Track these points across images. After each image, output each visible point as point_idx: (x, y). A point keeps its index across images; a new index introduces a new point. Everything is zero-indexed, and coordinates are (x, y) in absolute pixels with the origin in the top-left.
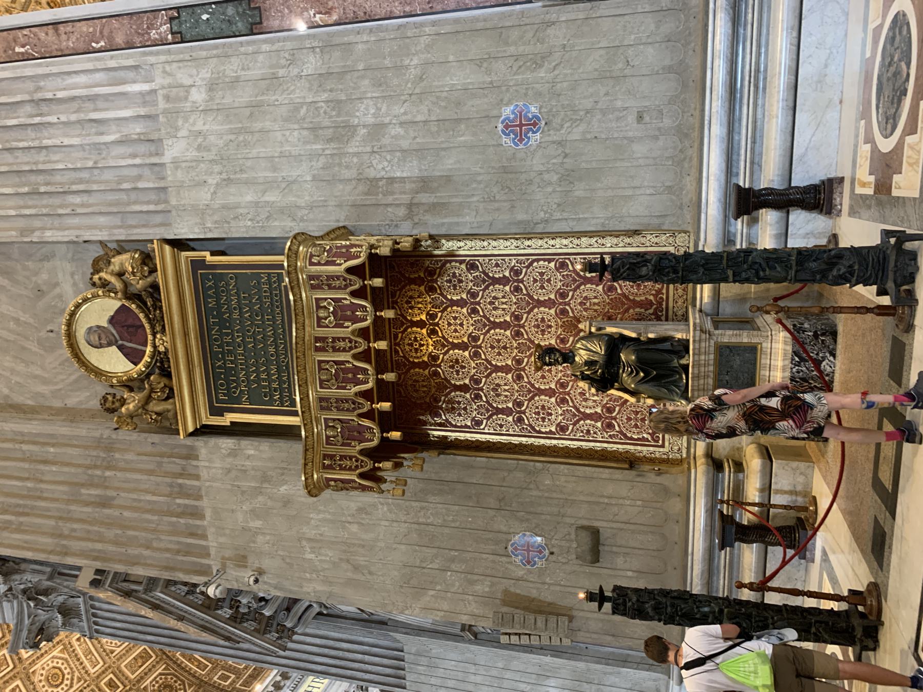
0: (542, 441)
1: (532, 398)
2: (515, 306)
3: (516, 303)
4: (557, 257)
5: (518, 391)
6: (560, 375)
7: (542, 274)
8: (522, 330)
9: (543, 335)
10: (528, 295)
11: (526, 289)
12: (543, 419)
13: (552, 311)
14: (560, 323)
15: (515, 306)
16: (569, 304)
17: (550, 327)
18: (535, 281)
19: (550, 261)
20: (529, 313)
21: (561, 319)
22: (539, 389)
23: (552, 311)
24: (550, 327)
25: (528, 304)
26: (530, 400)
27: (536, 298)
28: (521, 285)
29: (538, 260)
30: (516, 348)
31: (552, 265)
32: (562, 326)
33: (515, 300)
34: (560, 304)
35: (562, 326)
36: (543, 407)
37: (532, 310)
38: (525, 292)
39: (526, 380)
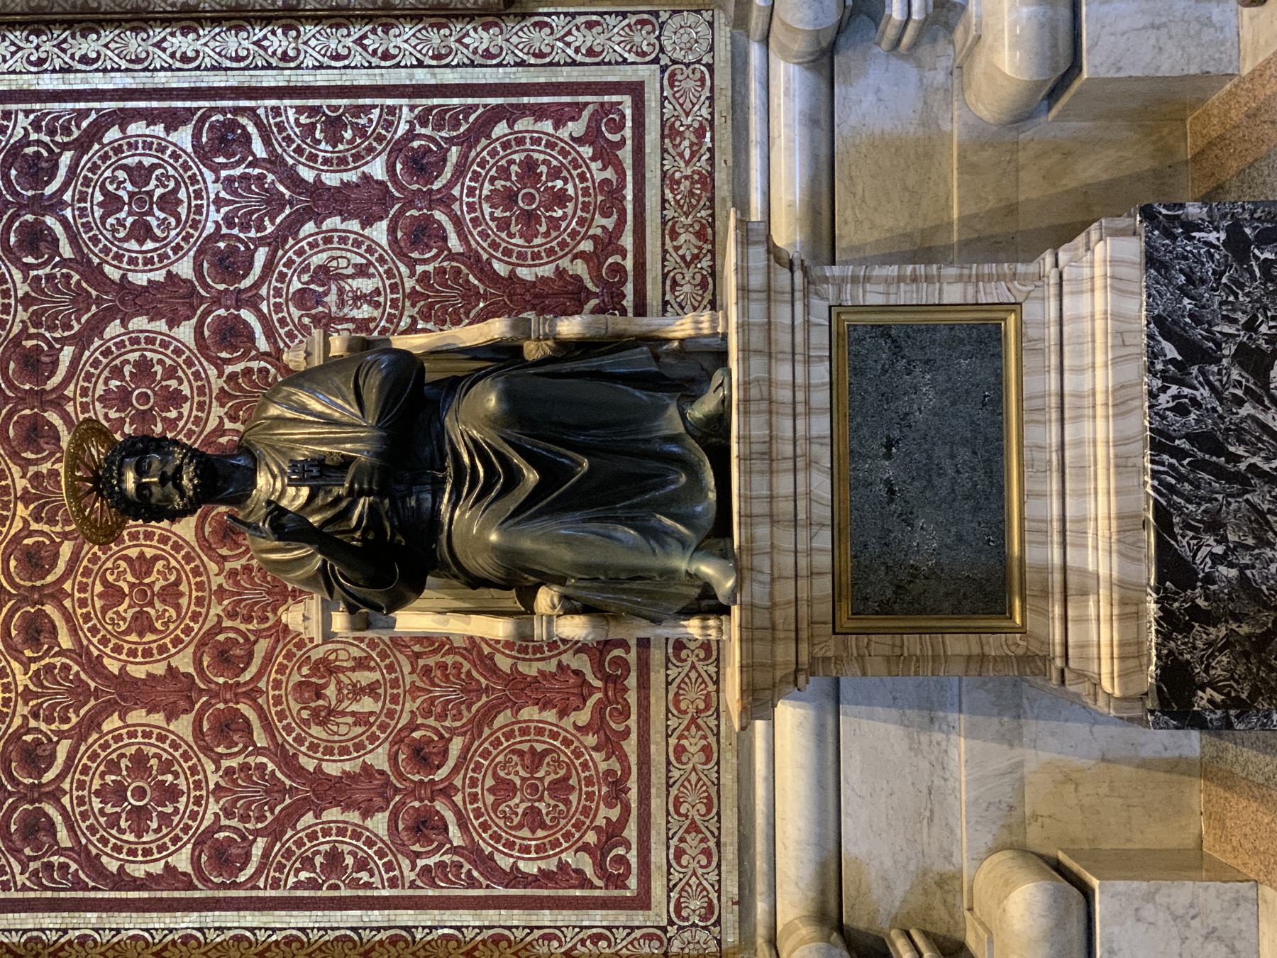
0: (132, 923)
1: (93, 723)
2: (22, 315)
3: (26, 301)
4: (207, 104)
5: (27, 695)
6: (216, 610)
7: (140, 174)
8: (53, 417)
10: (81, 262)
11: (74, 239)
12: (139, 815)
13: (185, 332)
14: (217, 383)
15: (22, 315)
16: (254, 305)
17: (176, 399)
18: (112, 203)
19: (173, 120)
20: (81, 342)
21: (219, 364)
22: (122, 680)
23: (185, 332)
24: (176, 399)
25: (81, 300)
26: (80, 734)
27: (113, 273)
28: (50, 220)
29: (122, 119)
30: (26, 498)
31: (183, 137)
32: (223, 396)
33: (22, 289)
34: (217, 301)
35: (223, 396)
36: (140, 761)
37: (96, 327)
38: (66, 251)
39: (65, 641)
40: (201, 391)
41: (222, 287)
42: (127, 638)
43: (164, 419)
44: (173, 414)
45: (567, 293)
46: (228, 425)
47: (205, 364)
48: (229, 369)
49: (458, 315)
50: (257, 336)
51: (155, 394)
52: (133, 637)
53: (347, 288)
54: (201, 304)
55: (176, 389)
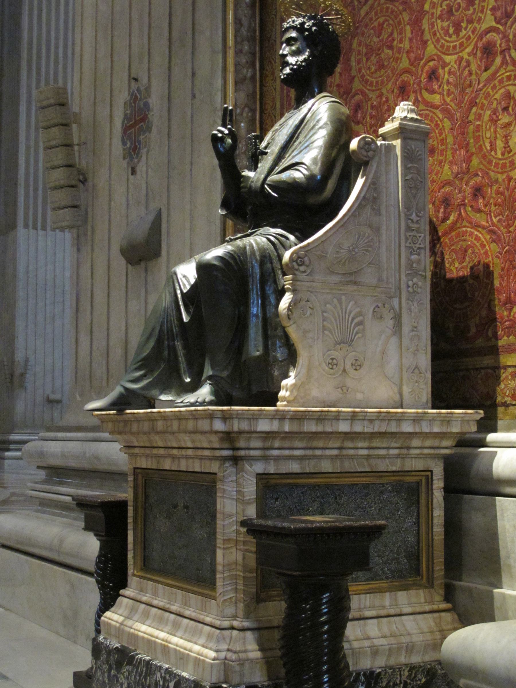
9: (440, 17)
40: (461, 45)
41: (511, 37)
42: (364, 48)
43: (449, 26)
44: (451, 30)
45: (510, 294)
46: (447, 69)
47: (474, 41)
48: (471, 58)
49: (499, 215)
50: (488, 71)
51: (460, 14)
52: (364, 51)
53: (511, 128)
54: (502, 25)
55: (462, 26)
